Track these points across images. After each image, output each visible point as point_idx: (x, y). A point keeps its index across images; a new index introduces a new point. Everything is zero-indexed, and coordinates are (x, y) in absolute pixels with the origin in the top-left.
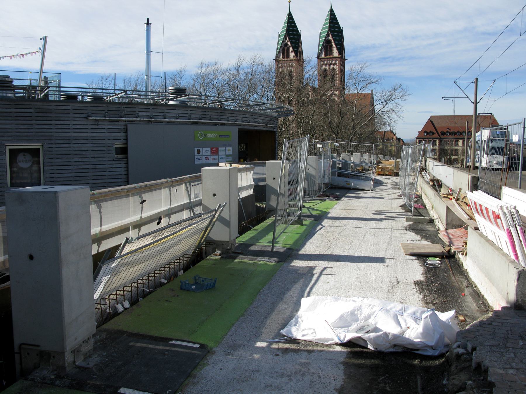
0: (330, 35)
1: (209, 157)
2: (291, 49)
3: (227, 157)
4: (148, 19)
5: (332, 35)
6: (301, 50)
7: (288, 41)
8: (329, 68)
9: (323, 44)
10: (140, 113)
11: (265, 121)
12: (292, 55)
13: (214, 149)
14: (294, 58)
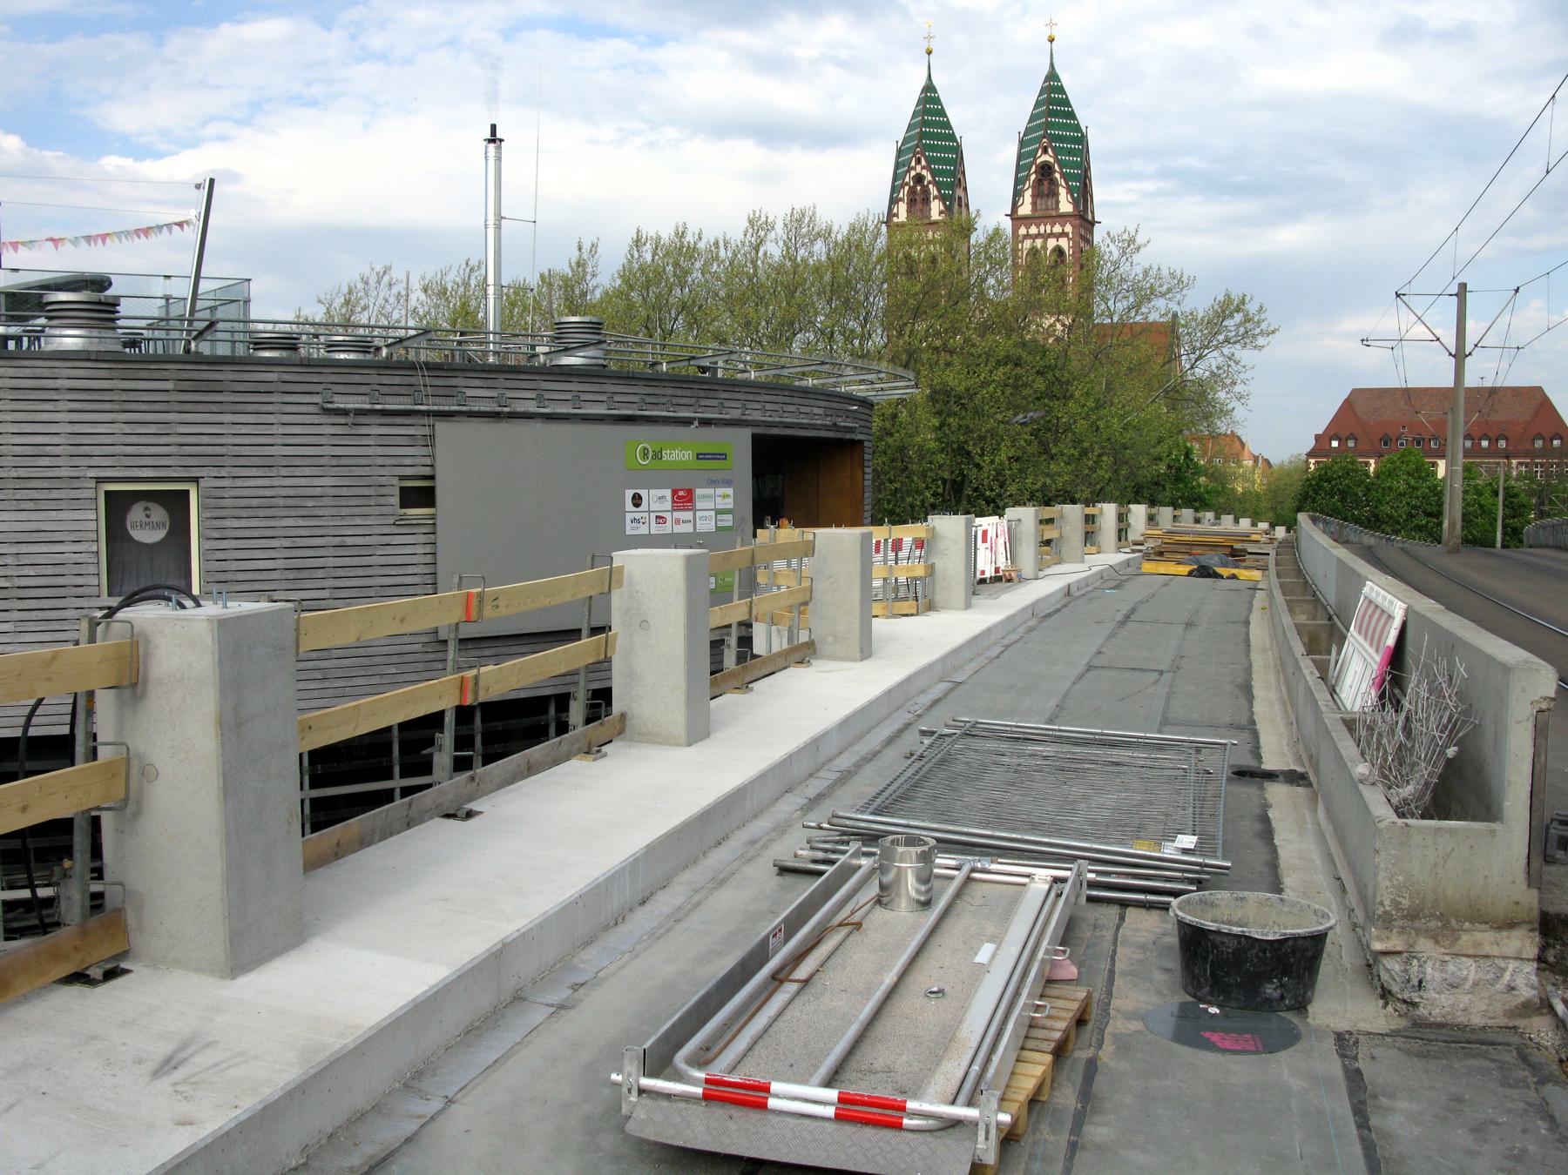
1: (667, 515)
2: (934, 191)
3: (719, 517)
4: (493, 128)
5: (1054, 149)
6: (962, 195)
10: (469, 392)
11: (830, 412)
12: (936, 208)
13: (681, 493)
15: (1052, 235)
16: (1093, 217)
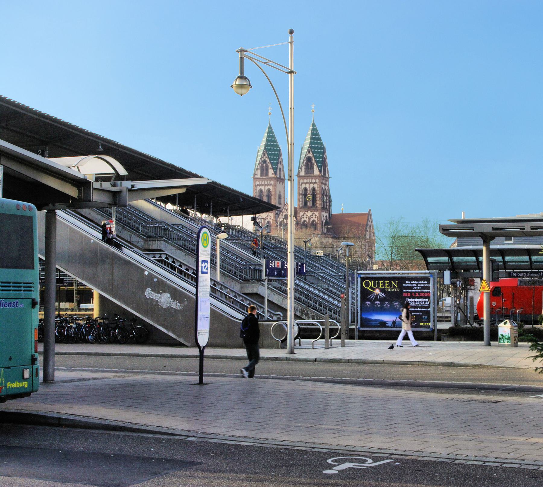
0: (311, 152)
2: (270, 166)
5: (312, 152)
7: (266, 157)
8: (309, 188)
9: (304, 161)
12: (271, 172)
14: (273, 176)
15: (311, 183)
16: (329, 176)
